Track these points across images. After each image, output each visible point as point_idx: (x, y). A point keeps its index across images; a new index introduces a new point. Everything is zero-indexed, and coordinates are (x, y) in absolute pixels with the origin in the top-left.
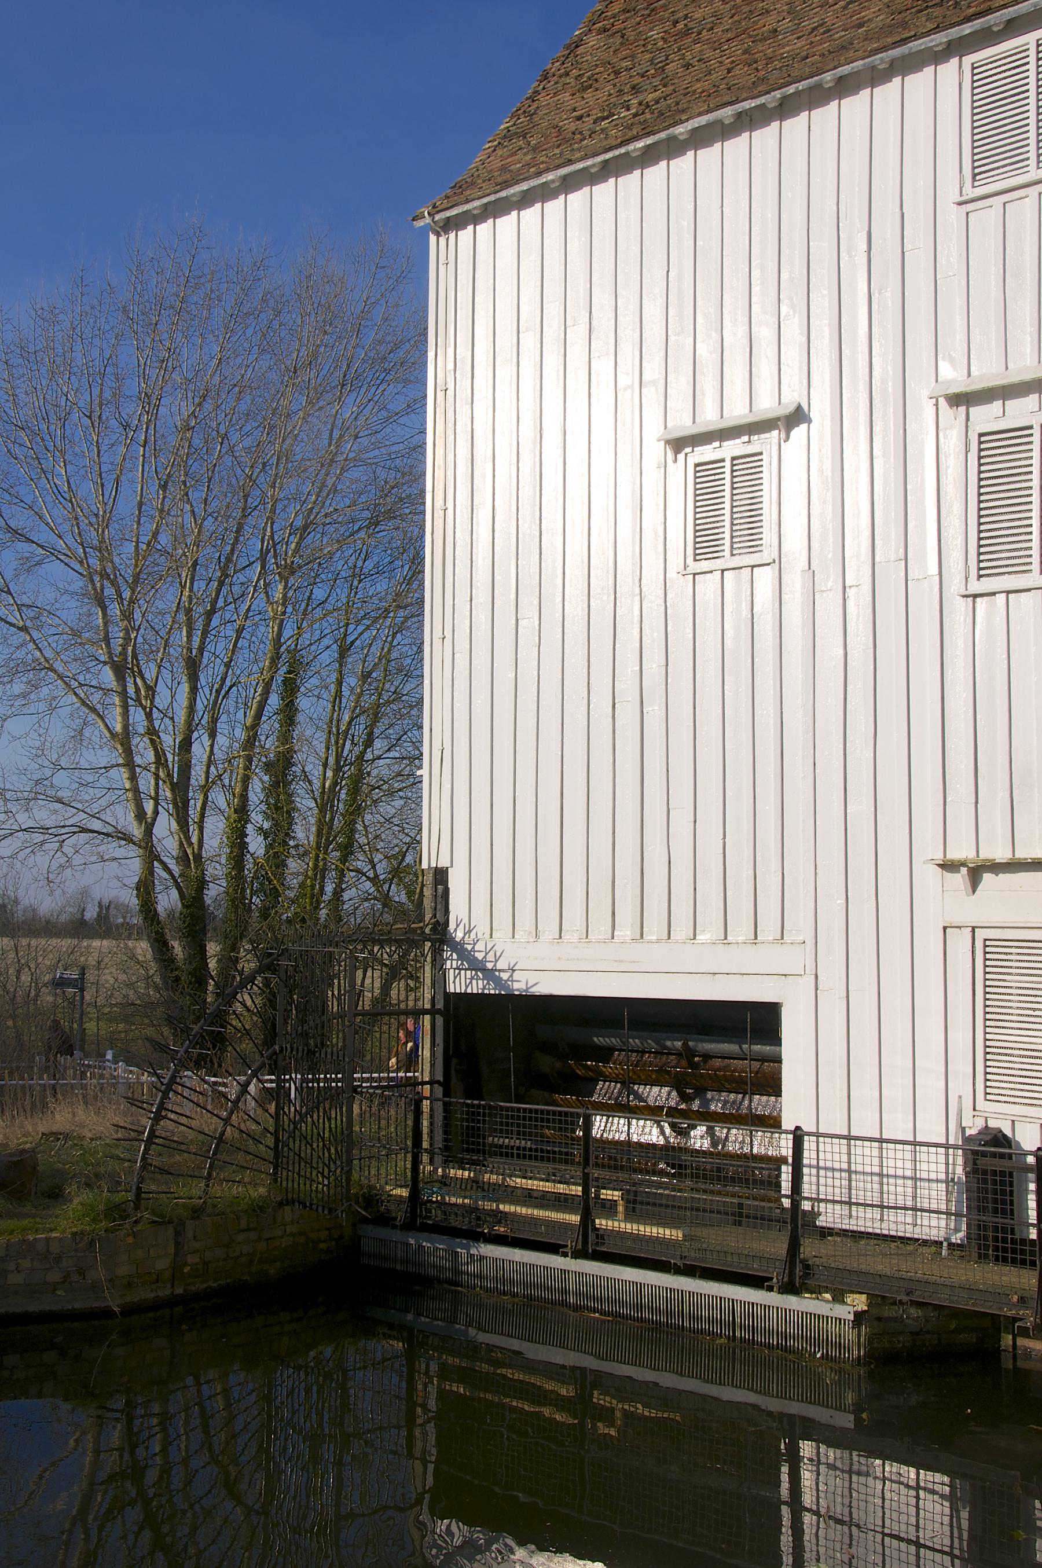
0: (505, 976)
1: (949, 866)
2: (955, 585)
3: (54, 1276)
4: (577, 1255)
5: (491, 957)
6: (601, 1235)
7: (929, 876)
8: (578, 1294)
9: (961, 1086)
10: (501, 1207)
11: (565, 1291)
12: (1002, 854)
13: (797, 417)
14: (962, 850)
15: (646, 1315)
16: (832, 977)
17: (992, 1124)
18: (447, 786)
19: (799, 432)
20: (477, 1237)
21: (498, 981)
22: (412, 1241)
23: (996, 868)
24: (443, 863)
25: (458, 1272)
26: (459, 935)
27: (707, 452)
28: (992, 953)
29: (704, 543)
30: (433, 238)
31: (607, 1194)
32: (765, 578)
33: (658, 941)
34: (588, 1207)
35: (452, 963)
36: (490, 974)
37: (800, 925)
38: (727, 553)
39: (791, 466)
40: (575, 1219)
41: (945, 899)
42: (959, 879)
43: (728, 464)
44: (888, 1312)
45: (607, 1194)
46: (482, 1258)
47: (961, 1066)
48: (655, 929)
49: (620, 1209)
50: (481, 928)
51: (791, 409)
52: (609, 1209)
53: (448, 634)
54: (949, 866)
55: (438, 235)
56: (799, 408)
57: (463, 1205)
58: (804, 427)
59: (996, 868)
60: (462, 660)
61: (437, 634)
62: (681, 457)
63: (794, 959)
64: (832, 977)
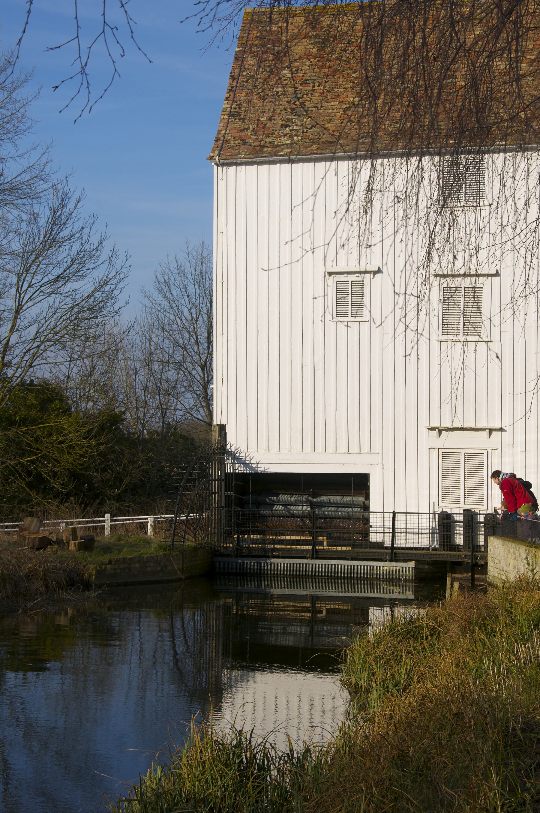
0: (254, 466)
1: (433, 429)
2: (434, 337)
3: (159, 569)
4: (312, 558)
5: (248, 458)
6: (317, 552)
7: (424, 431)
8: (312, 571)
9: (434, 499)
10: (276, 546)
11: (307, 571)
12: (449, 425)
13: (379, 271)
14: (435, 424)
15: (339, 575)
16: (389, 465)
17: (444, 510)
18: (225, 392)
19: (378, 276)
20: (269, 557)
21: (251, 468)
22: (240, 561)
23: (447, 430)
24: (224, 422)
25: (260, 569)
26: (233, 449)
27: (342, 278)
28: (446, 457)
29: (340, 311)
30: (215, 167)
31: (320, 538)
32: (365, 327)
33: (322, 452)
34: (314, 543)
35: (228, 462)
36: (246, 465)
37: (377, 446)
38: (349, 315)
39: (373, 287)
40: (310, 547)
41: (430, 440)
42: (436, 433)
43: (350, 283)
44: (420, 566)
45: (320, 538)
46: (271, 563)
47: (434, 492)
48: (320, 447)
49: (325, 542)
50: (242, 447)
51: (377, 269)
52: (321, 543)
53: (225, 332)
54: (433, 429)
55: (218, 166)
56: (379, 267)
57: (258, 548)
58: (380, 275)
59: (447, 430)
60: (232, 344)
61: (220, 331)
62: (331, 277)
63: (376, 459)
64: (389, 465)
